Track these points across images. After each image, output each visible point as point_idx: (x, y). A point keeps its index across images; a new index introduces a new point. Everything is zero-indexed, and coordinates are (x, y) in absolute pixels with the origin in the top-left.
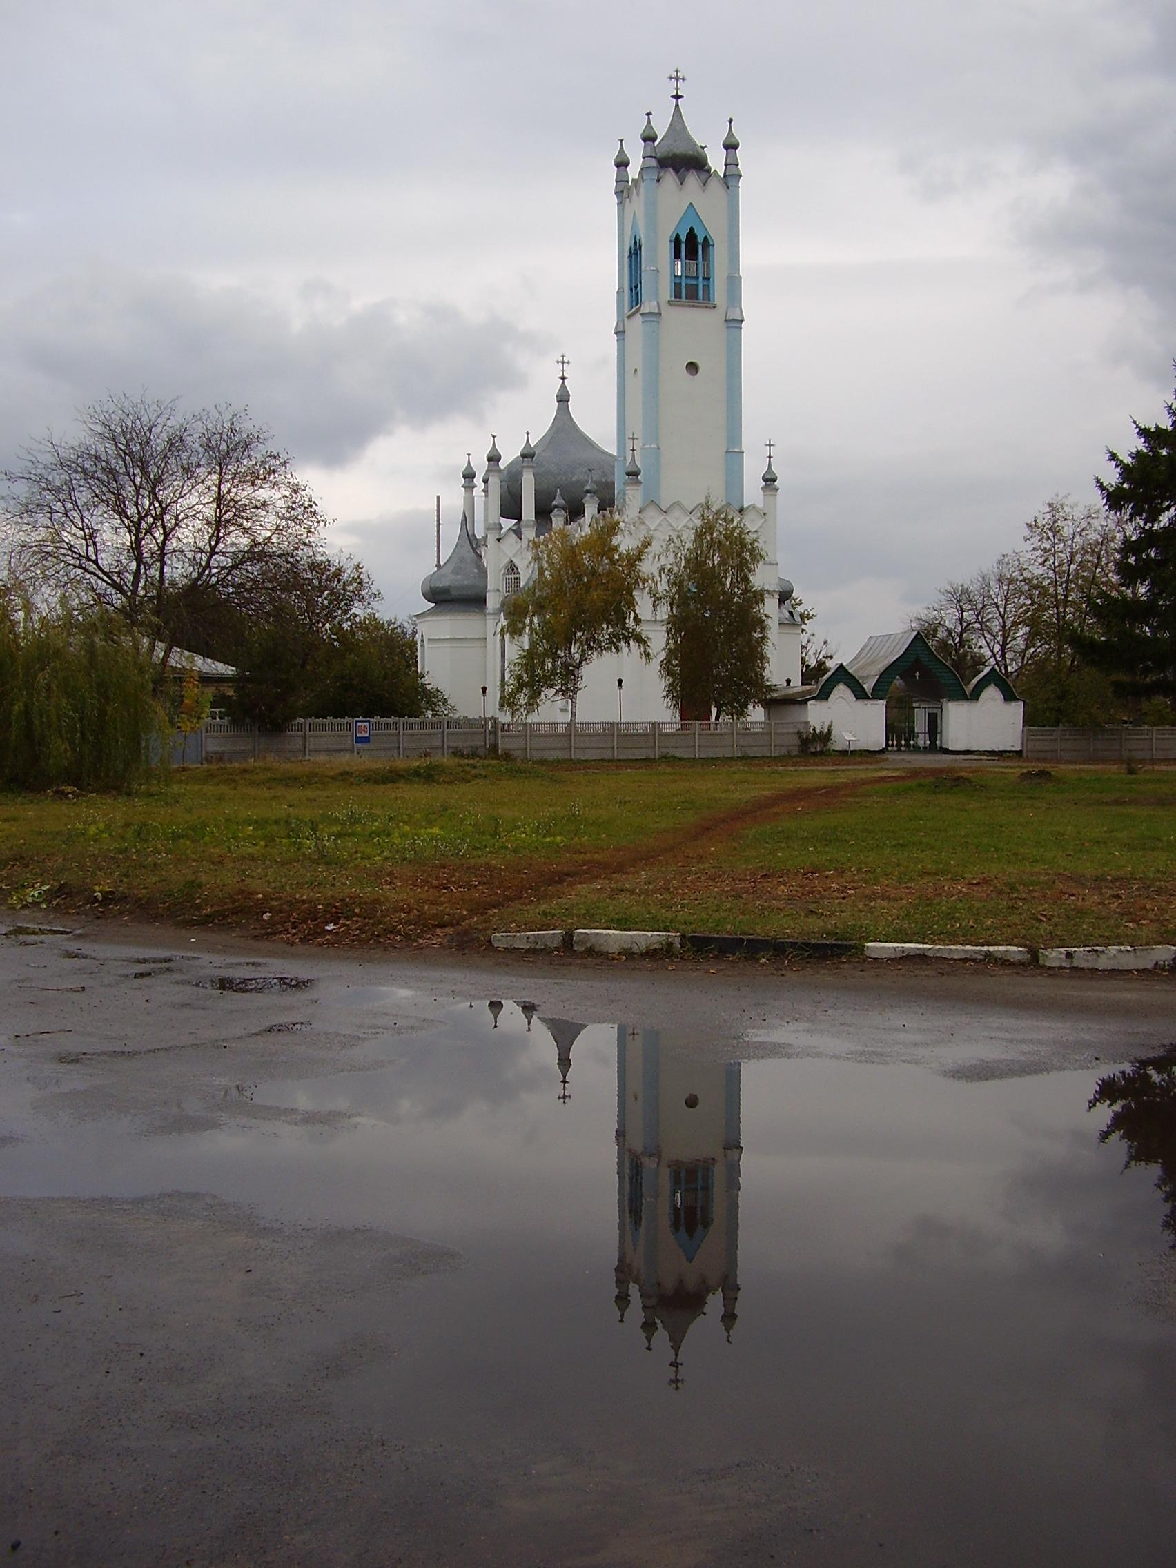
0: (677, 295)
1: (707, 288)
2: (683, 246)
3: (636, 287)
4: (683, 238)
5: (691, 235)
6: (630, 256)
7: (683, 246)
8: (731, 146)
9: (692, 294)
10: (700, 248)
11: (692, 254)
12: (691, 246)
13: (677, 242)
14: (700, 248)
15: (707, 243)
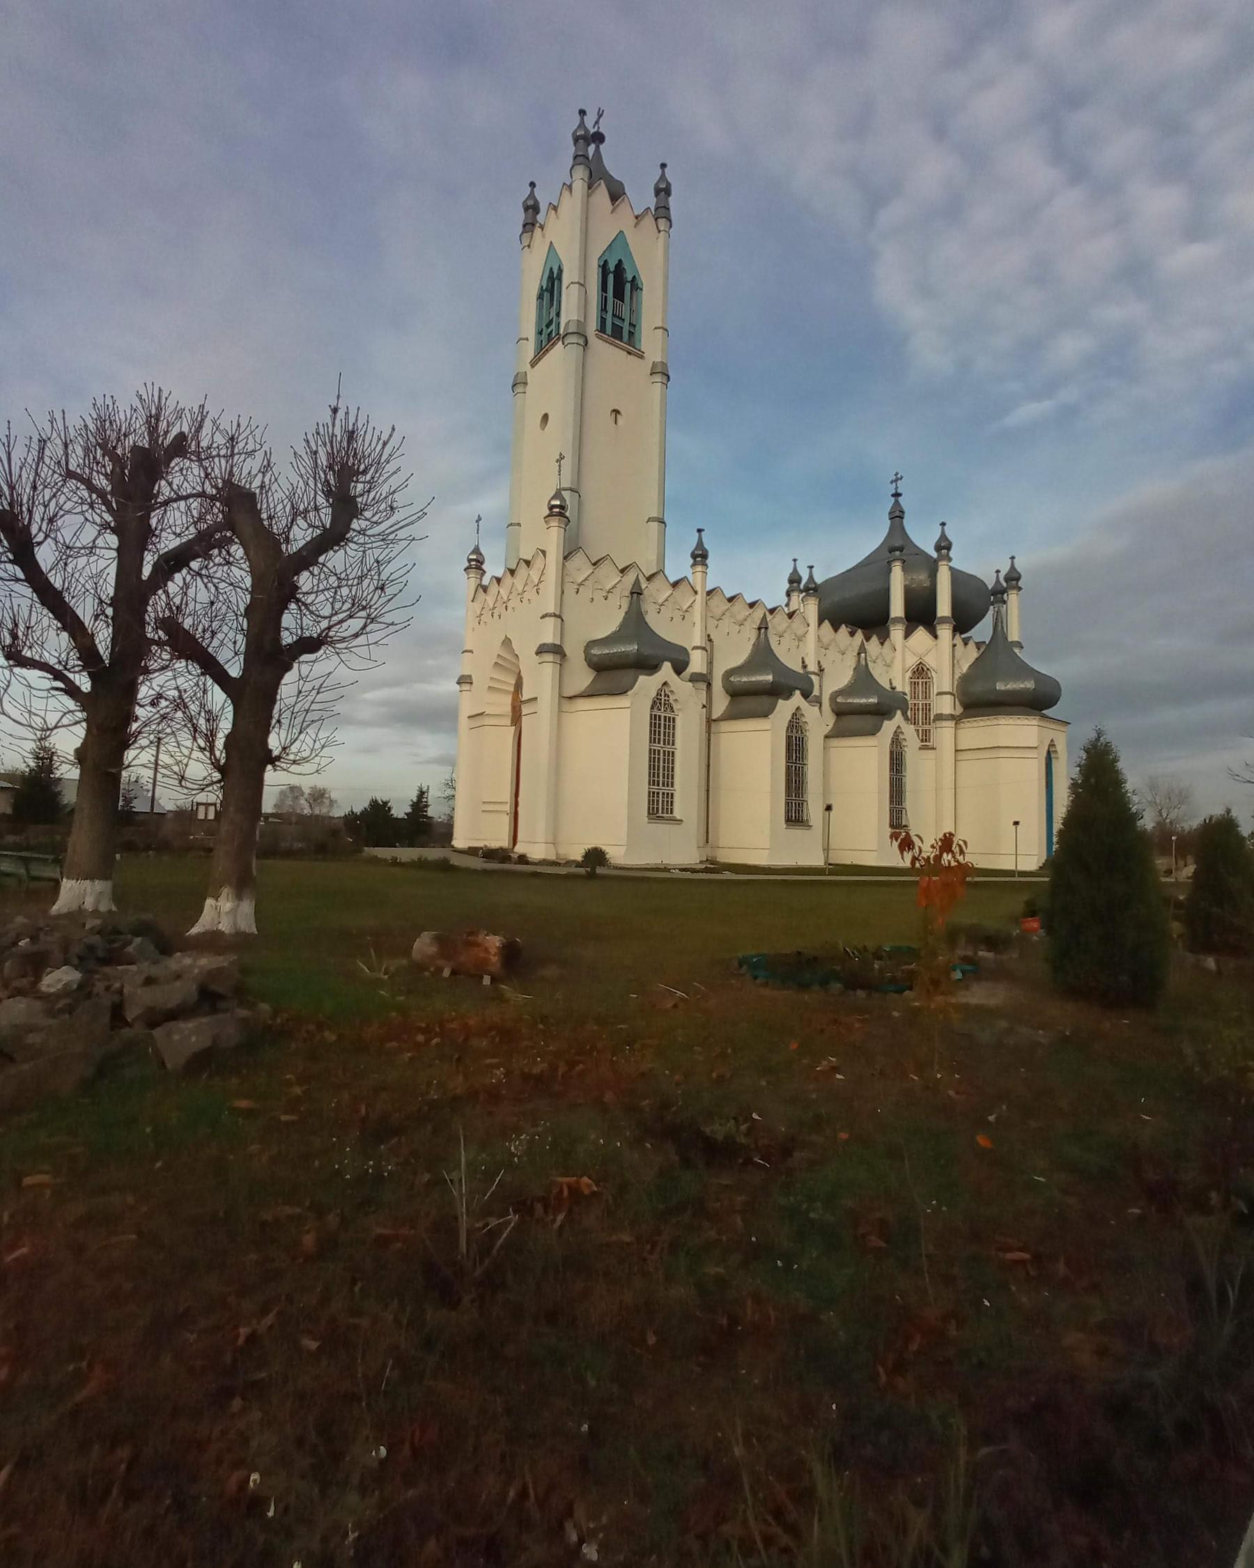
0: (602, 329)
1: (631, 334)
2: (611, 278)
3: (550, 322)
4: (612, 269)
5: (619, 264)
6: (540, 297)
7: (611, 278)
8: (663, 191)
9: (617, 333)
10: (628, 286)
11: (619, 294)
12: (618, 282)
13: (604, 267)
14: (628, 286)
15: (635, 286)
